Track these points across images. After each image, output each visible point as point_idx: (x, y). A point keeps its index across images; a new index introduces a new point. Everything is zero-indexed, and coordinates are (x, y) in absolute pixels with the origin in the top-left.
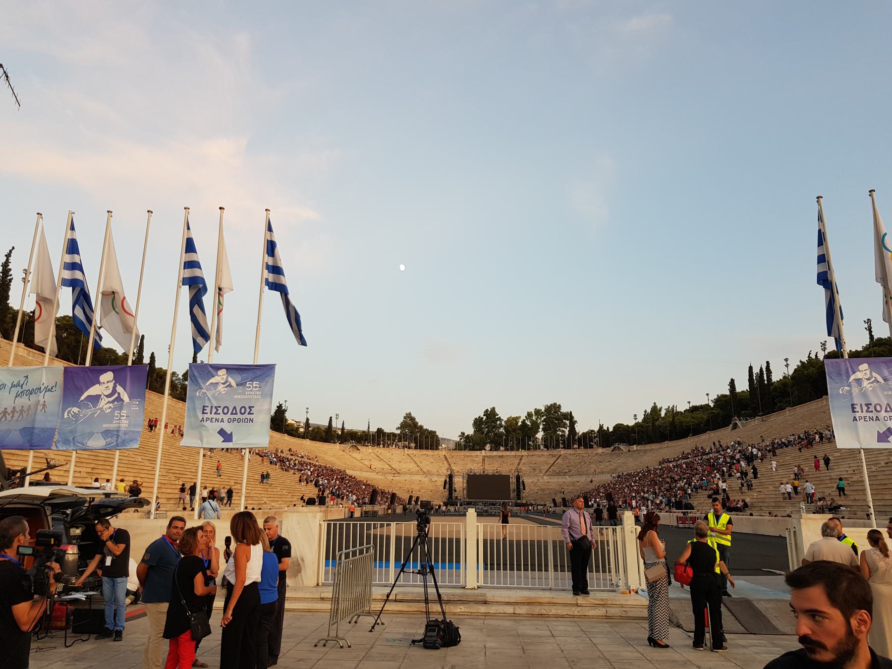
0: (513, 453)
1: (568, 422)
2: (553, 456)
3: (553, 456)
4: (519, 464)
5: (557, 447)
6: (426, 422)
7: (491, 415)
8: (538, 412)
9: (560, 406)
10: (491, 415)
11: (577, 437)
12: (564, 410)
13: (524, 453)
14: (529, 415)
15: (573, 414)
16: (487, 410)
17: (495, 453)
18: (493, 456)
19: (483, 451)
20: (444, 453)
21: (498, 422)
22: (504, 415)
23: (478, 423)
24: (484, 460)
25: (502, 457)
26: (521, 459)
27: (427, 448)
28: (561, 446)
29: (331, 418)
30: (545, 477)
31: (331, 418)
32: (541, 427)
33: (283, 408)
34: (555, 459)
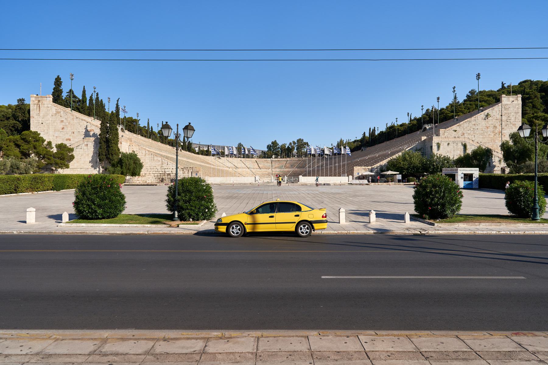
0: (284, 159)
4: (286, 163)
13: (288, 159)
17: (276, 159)
18: (276, 161)
19: (272, 159)
24: (272, 162)
26: (287, 162)
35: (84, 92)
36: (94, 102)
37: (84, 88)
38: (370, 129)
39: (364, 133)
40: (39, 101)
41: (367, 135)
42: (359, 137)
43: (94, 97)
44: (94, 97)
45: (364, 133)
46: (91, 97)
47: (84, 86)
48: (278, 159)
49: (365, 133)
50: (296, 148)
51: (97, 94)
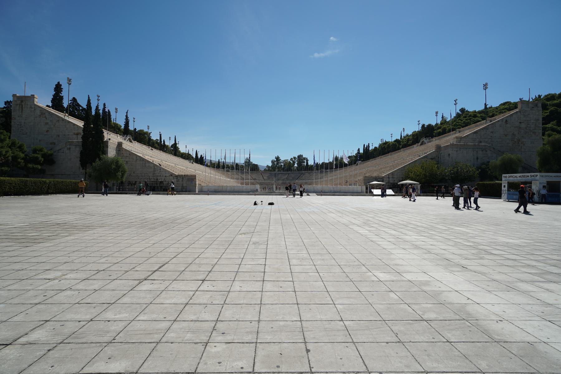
1: (306, 161)
2: (300, 173)
3: (300, 173)
5: (301, 170)
6: (254, 161)
7: (278, 159)
8: (295, 158)
9: (302, 155)
10: (278, 159)
11: (308, 167)
12: (304, 157)
13: (289, 172)
14: (291, 159)
15: (308, 159)
16: (276, 157)
17: (279, 172)
20: (261, 172)
21: (280, 161)
22: (282, 158)
23: (273, 162)
24: (275, 175)
25: (281, 174)
27: (254, 170)
28: (303, 170)
29: (219, 160)
30: (297, 181)
31: (219, 160)
32: (296, 163)
33: (203, 156)
34: (300, 174)
35: (89, 101)
36: (101, 112)
37: (89, 97)
38: (364, 145)
39: (359, 150)
40: (22, 101)
41: (361, 151)
42: (354, 153)
43: (101, 108)
44: (101, 108)
45: (359, 150)
46: (97, 107)
47: (89, 95)
48: (281, 172)
49: (359, 149)
50: (296, 163)
51: (104, 104)
